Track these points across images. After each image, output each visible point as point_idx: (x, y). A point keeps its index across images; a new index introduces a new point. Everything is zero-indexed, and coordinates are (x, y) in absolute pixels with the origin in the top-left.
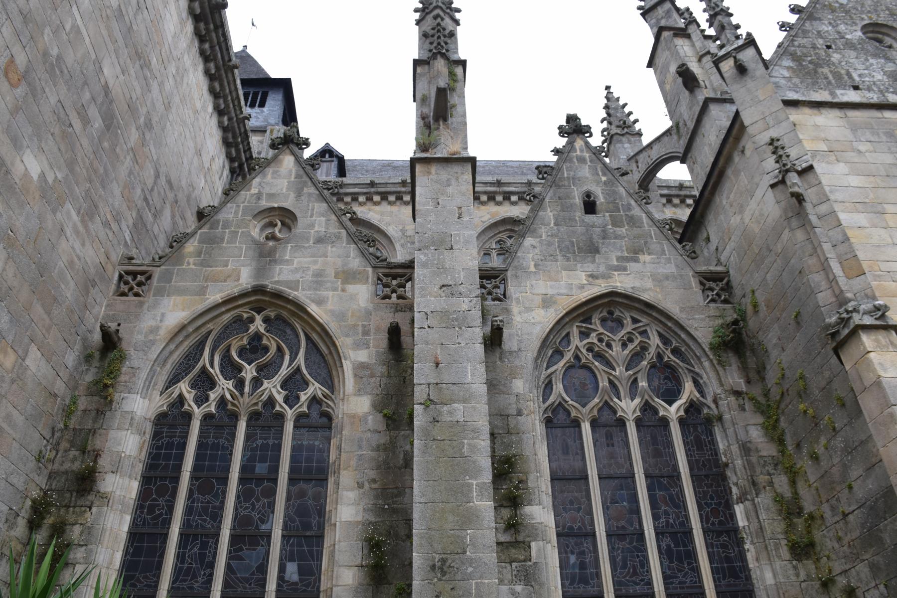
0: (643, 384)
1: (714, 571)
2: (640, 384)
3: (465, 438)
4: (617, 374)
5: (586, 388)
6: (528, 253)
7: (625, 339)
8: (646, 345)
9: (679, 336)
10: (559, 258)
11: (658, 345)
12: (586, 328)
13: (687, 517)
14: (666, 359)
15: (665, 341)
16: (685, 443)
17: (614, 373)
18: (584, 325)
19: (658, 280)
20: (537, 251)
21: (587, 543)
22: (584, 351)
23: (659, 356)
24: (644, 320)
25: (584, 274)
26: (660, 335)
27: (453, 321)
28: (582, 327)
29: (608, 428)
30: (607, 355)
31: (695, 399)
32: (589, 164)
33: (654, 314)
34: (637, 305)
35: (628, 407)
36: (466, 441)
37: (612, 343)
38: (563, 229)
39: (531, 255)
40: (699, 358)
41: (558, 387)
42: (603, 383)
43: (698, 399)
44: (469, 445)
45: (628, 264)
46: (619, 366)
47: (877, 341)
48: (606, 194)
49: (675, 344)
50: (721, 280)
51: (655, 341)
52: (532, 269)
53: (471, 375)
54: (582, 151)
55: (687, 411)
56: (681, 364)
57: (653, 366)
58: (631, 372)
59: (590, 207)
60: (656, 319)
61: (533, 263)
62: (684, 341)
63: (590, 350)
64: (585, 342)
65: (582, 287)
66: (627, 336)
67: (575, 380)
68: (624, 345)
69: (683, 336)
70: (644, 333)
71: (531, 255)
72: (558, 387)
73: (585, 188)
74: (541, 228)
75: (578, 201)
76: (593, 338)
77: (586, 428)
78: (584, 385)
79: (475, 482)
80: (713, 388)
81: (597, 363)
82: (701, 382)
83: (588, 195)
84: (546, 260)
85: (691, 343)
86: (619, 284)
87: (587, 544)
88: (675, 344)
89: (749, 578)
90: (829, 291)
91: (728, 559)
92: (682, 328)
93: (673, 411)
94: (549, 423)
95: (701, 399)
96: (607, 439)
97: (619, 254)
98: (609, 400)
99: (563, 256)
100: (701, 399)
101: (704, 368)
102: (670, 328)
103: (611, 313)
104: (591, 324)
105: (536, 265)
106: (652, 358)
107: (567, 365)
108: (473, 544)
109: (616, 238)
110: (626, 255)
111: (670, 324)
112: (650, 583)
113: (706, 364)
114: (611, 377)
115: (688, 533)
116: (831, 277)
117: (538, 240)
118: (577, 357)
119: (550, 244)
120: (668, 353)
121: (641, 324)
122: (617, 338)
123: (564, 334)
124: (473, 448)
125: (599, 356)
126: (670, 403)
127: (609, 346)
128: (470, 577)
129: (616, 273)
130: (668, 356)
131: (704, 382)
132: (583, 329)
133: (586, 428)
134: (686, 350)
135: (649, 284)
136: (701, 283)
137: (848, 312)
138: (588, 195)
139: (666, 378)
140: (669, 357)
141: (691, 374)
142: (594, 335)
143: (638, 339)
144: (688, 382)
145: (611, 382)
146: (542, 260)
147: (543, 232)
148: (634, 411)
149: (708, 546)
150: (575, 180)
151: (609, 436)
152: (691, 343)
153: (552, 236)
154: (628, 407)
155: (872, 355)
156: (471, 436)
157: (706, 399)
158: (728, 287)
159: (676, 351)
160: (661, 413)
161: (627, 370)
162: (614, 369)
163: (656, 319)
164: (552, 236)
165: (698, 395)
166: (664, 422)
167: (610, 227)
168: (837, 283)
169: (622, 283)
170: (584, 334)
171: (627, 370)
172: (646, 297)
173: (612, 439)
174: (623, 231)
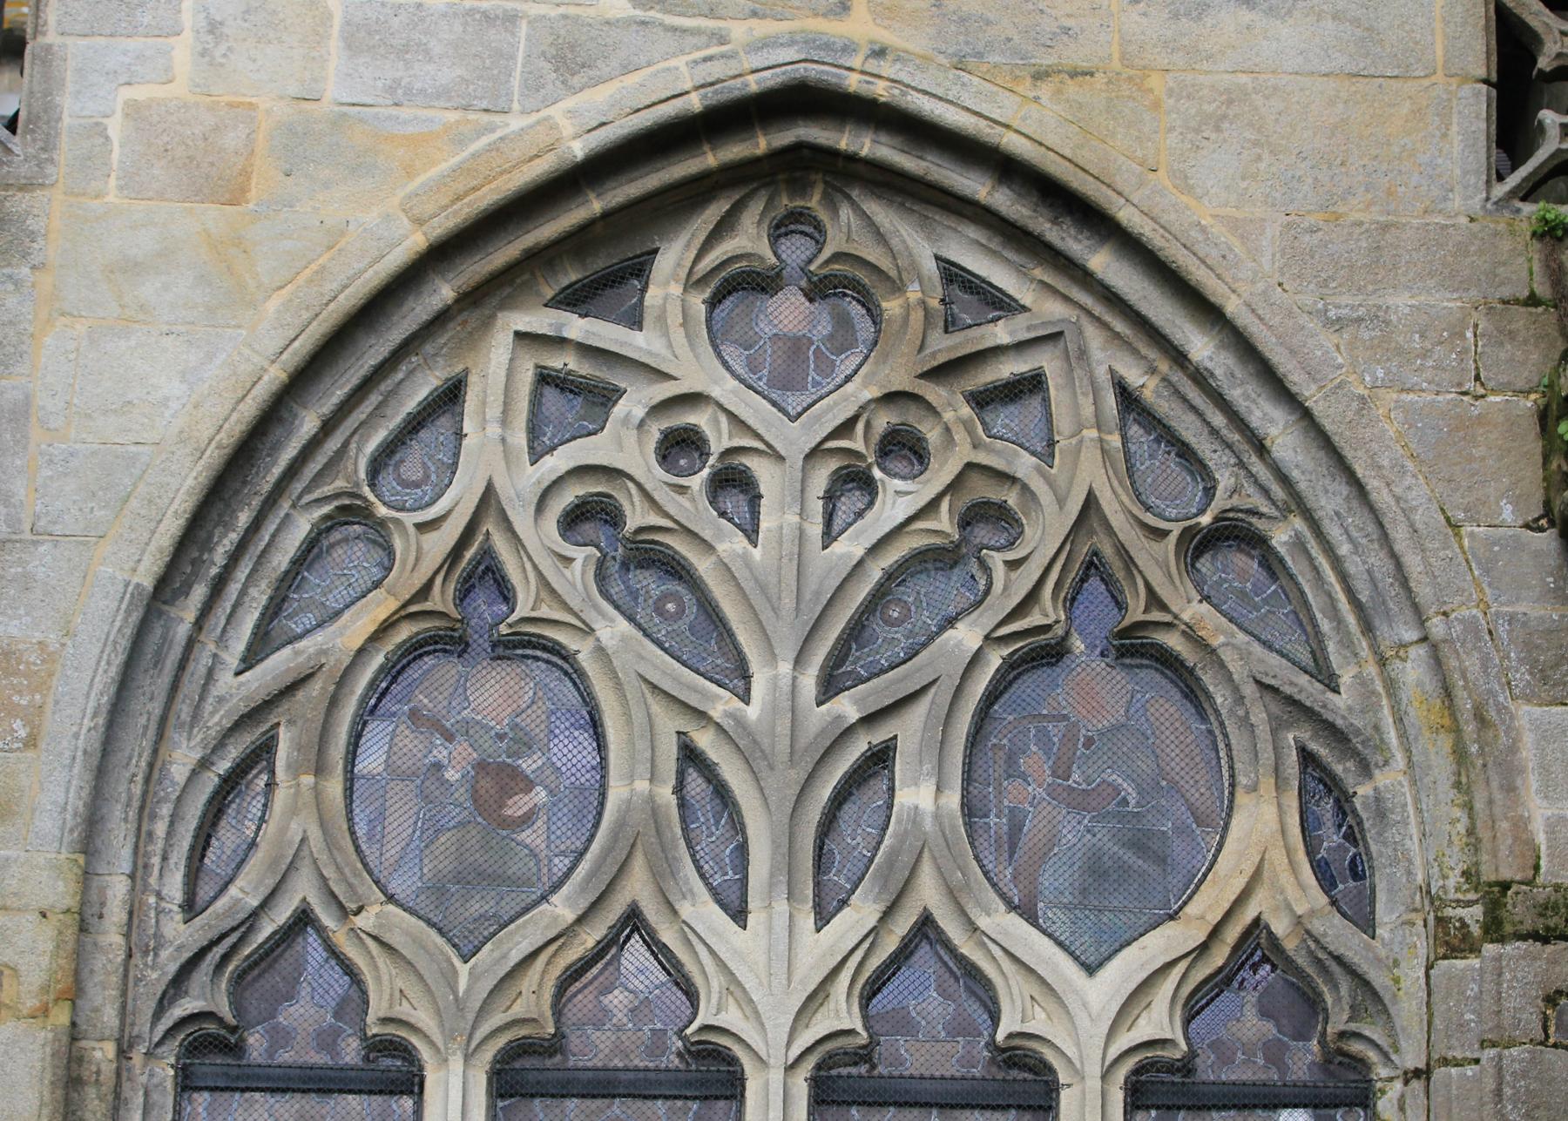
4: (753, 712)
5: (518, 806)
7: (857, 444)
8: (1012, 498)
17: (722, 704)
31: (1280, 926)
37: (760, 469)
46: (772, 657)
58: (847, 707)
60: (1113, 299)
66: (883, 421)
81: (613, 629)
82: (1364, 790)
98: (652, 912)
104: (635, 320)
106: (1031, 598)
107: (405, 632)
114: (704, 740)
122: (796, 438)
123: (421, 388)
132: (558, 361)
134: (1299, 544)
140: (1154, 601)
144: (1253, 788)
148: (817, 997)
157: (1367, 924)
161: (830, 686)
162: (739, 677)
165: (1308, 896)
171: (830, 686)
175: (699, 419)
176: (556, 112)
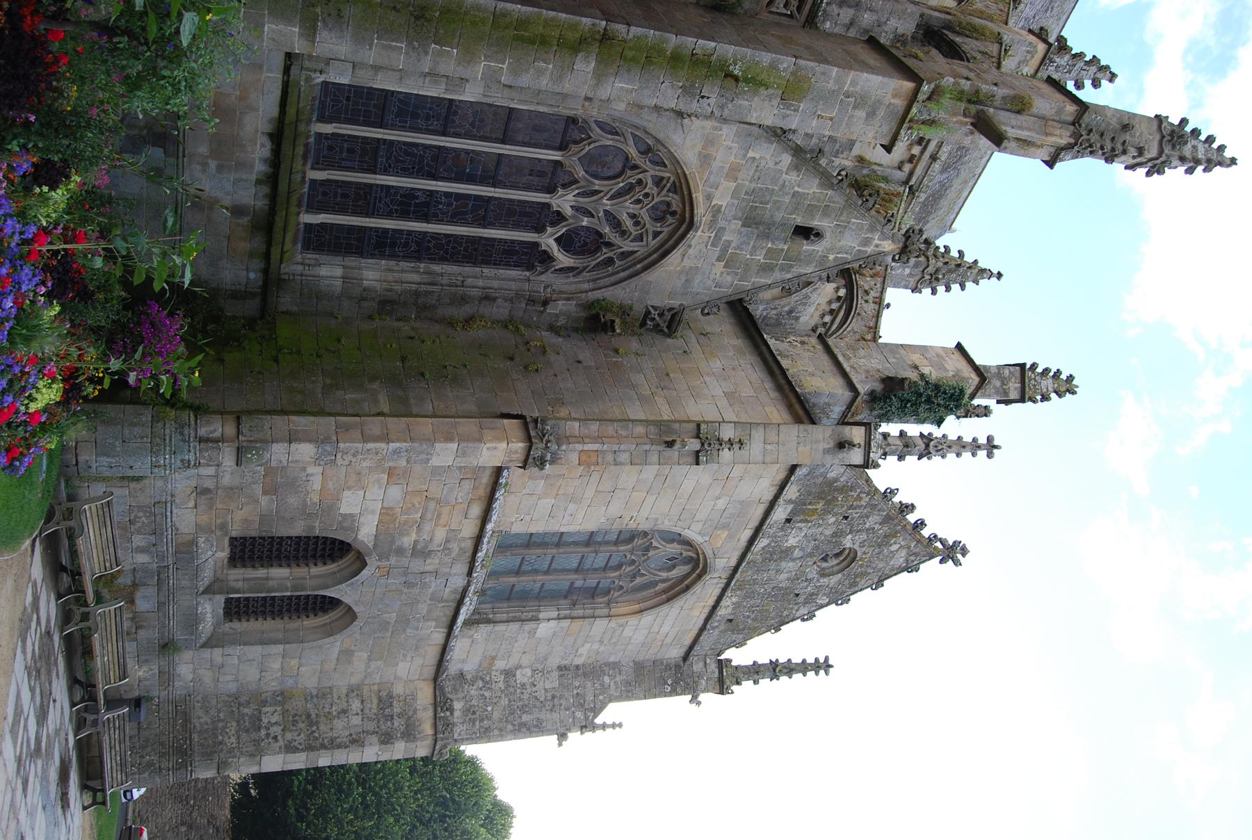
0: (585, 222)
1: (386, 231)
2: (586, 219)
3: (553, 67)
6: (772, 155)
8: (626, 237)
9: (623, 270)
10: (753, 185)
11: (621, 247)
12: (665, 186)
13: (440, 221)
14: (604, 250)
15: (624, 255)
16: (513, 242)
18: (669, 185)
19: (690, 274)
20: (771, 165)
21: (437, 125)
22: (640, 176)
23: (609, 245)
24: (653, 243)
25: (724, 204)
26: (633, 252)
27: (692, 81)
28: (668, 182)
29: (550, 175)
30: (628, 197)
32: (857, 248)
33: (655, 256)
34: (671, 243)
35: (564, 202)
36: (551, 67)
37: (640, 206)
38: (787, 199)
39: (768, 157)
40: (594, 280)
41: (608, 141)
42: (598, 184)
43: (554, 266)
44: (546, 69)
45: (718, 249)
46: (611, 205)
47: (516, 452)
48: (811, 254)
49: (618, 263)
50: (669, 327)
51: (627, 246)
52: (751, 154)
53: (622, 87)
54: (877, 246)
55: (545, 252)
56: (594, 263)
57: (600, 235)
58: (601, 214)
59: (805, 232)
60: (650, 255)
61: (757, 156)
62: (618, 272)
63: (640, 182)
64: (650, 181)
65: (709, 197)
67: (610, 158)
68: (633, 216)
69: (622, 275)
70: (640, 238)
71: (768, 157)
72: (608, 141)
73: (828, 234)
74: (798, 176)
75: (815, 223)
76: (651, 188)
77: (555, 155)
78: (604, 165)
79: (505, 66)
80: (560, 283)
82: (571, 274)
83: (818, 235)
84: (756, 171)
85: (613, 279)
86: (699, 233)
87: (436, 124)
88: (618, 263)
89: (373, 256)
90: (577, 433)
91: (393, 245)
92: (630, 277)
93: (548, 241)
94: (572, 121)
95: (553, 269)
96: (538, 171)
97: (733, 245)
99: (754, 189)
100: (553, 269)
101: (583, 282)
102: (635, 264)
103: (673, 213)
104: (669, 191)
105: (754, 159)
107: (630, 156)
108: (440, 54)
109: (754, 247)
110: (730, 251)
111: (639, 266)
112: (386, 172)
113: (586, 286)
114: (602, 194)
115: (426, 218)
116: (586, 440)
117: (785, 170)
118: (635, 167)
119: (774, 180)
120: (610, 254)
121: (650, 238)
124: (540, 72)
125: (629, 189)
126: (558, 240)
127: (638, 201)
128: (410, 43)
129: (713, 235)
130: (605, 253)
131: (569, 277)
132: (664, 182)
133: (555, 155)
135: (687, 263)
136: (671, 309)
137: (548, 441)
138: (818, 235)
139: (586, 244)
140: (605, 253)
141: (581, 268)
142: (655, 191)
143: (634, 231)
145: (597, 192)
146: (757, 166)
147: (793, 177)
149: (410, 233)
150: (841, 229)
151: (541, 174)
152: (613, 279)
153: (783, 186)
154: (564, 202)
155: (504, 445)
156: (554, 73)
158: (657, 329)
159: (610, 261)
160: (549, 230)
161: (605, 211)
162: (611, 198)
163: (650, 255)
164: (783, 186)
166: (540, 229)
167: (770, 245)
168: (579, 443)
169: (698, 238)
170: (659, 182)
171: (605, 211)
172: (675, 255)
173: (537, 176)
174: (760, 257)
175: (650, 198)
176: (700, 193)
